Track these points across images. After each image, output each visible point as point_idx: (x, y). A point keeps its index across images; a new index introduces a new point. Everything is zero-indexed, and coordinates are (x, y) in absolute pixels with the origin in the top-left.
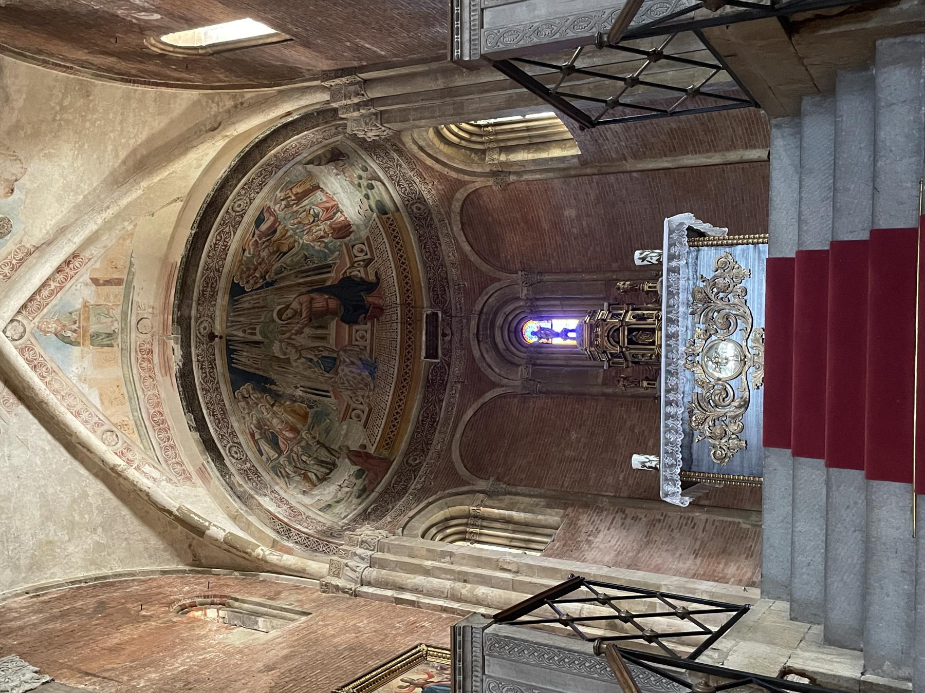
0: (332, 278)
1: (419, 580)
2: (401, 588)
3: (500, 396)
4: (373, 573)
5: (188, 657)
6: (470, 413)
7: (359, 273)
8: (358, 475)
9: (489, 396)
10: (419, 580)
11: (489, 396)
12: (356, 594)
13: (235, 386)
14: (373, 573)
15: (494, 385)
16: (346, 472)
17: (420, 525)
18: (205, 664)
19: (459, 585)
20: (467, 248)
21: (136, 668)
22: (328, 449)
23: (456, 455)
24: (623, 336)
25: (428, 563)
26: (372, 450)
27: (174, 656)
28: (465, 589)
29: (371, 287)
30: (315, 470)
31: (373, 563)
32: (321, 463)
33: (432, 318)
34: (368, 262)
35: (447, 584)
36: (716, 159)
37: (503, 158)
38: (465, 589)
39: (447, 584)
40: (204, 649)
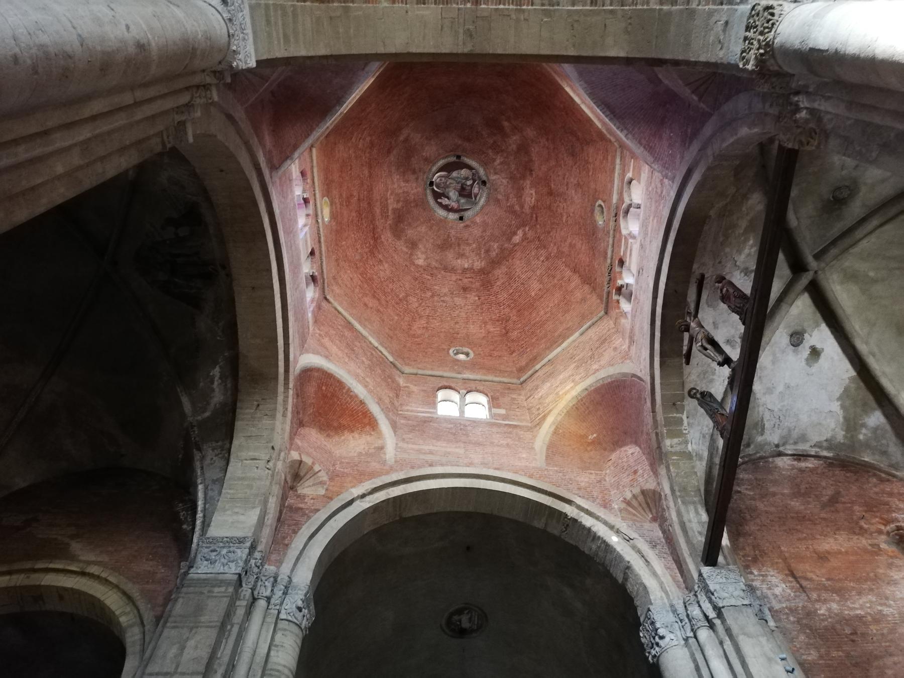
5: (871, 602)
18: (878, 619)
21: (826, 589)
27: (859, 593)
40: (887, 598)
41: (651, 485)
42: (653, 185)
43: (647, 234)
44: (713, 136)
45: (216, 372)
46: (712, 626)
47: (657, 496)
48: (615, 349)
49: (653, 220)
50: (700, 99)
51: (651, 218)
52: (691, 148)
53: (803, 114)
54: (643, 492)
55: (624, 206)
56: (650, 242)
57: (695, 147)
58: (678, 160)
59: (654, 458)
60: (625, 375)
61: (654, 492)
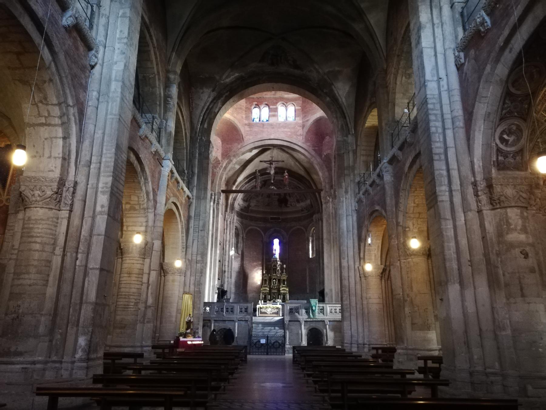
0: (288, 197)
1: (228, 233)
2: (227, 229)
3: (262, 236)
4: (228, 223)
6: (259, 229)
7: (289, 203)
8: (245, 207)
9: (262, 233)
10: (228, 233)
11: (262, 233)
12: (225, 220)
13: (263, 181)
14: (228, 223)
15: (265, 234)
16: (246, 204)
17: (237, 225)
19: (228, 241)
20: (294, 228)
22: (250, 200)
23: (250, 228)
24: (275, 267)
25: (231, 234)
26: (250, 208)
28: (228, 243)
29: (286, 205)
30: (246, 198)
31: (230, 222)
32: (247, 199)
33: (279, 219)
34: (291, 205)
35: (228, 239)
36: (307, 283)
37: (311, 241)
38: (228, 243)
39: (228, 239)
41: (220, 158)
42: (298, 128)
43: (284, 128)
44: (317, 161)
45: (237, 75)
46: (214, 203)
47: (218, 162)
48: (242, 117)
49: (289, 132)
50: (325, 156)
51: (289, 130)
52: (313, 151)
53: (328, 198)
54: (217, 158)
55: (285, 103)
56: (283, 131)
57: (313, 153)
58: (308, 144)
59: (227, 155)
60: (240, 131)
61: (219, 161)
